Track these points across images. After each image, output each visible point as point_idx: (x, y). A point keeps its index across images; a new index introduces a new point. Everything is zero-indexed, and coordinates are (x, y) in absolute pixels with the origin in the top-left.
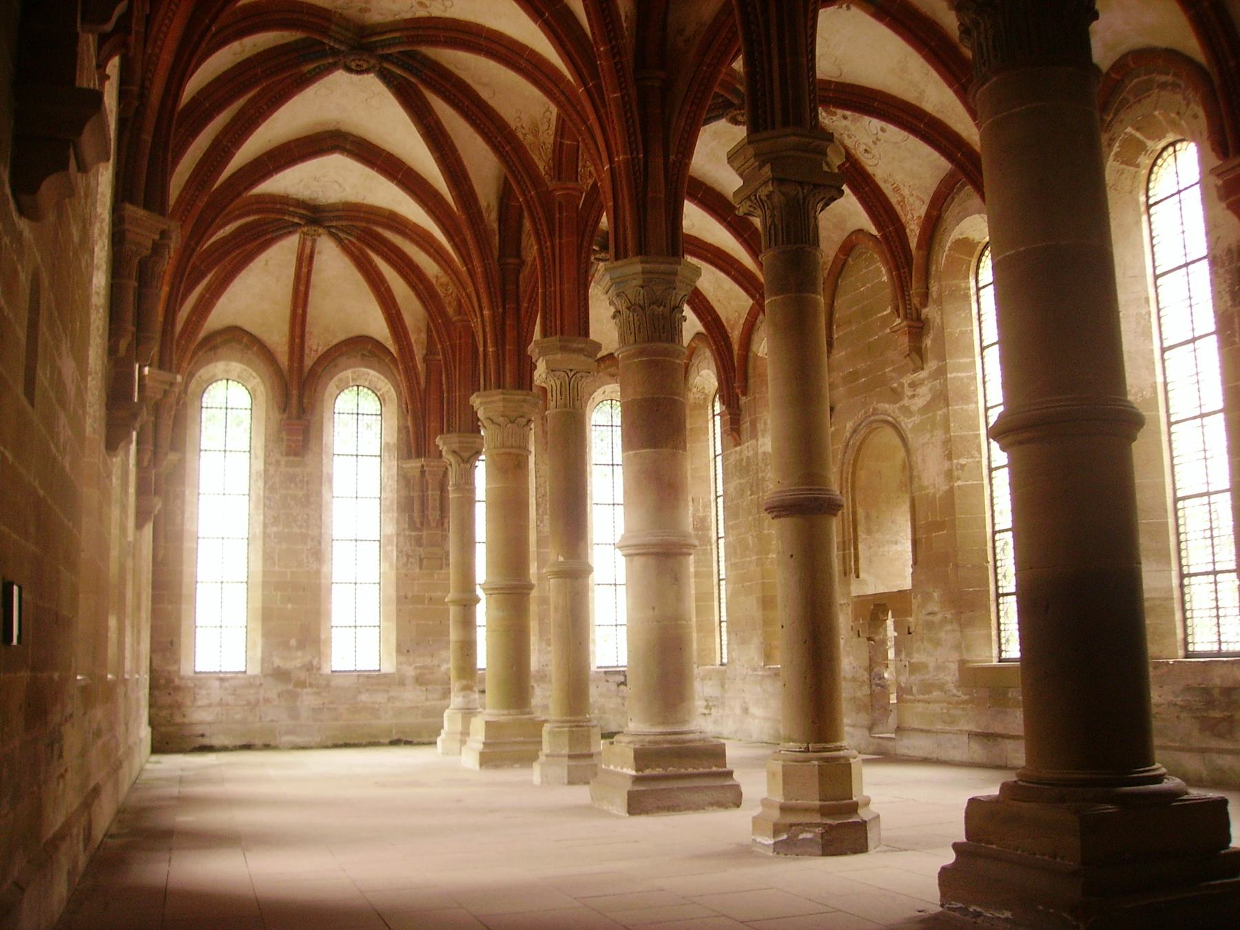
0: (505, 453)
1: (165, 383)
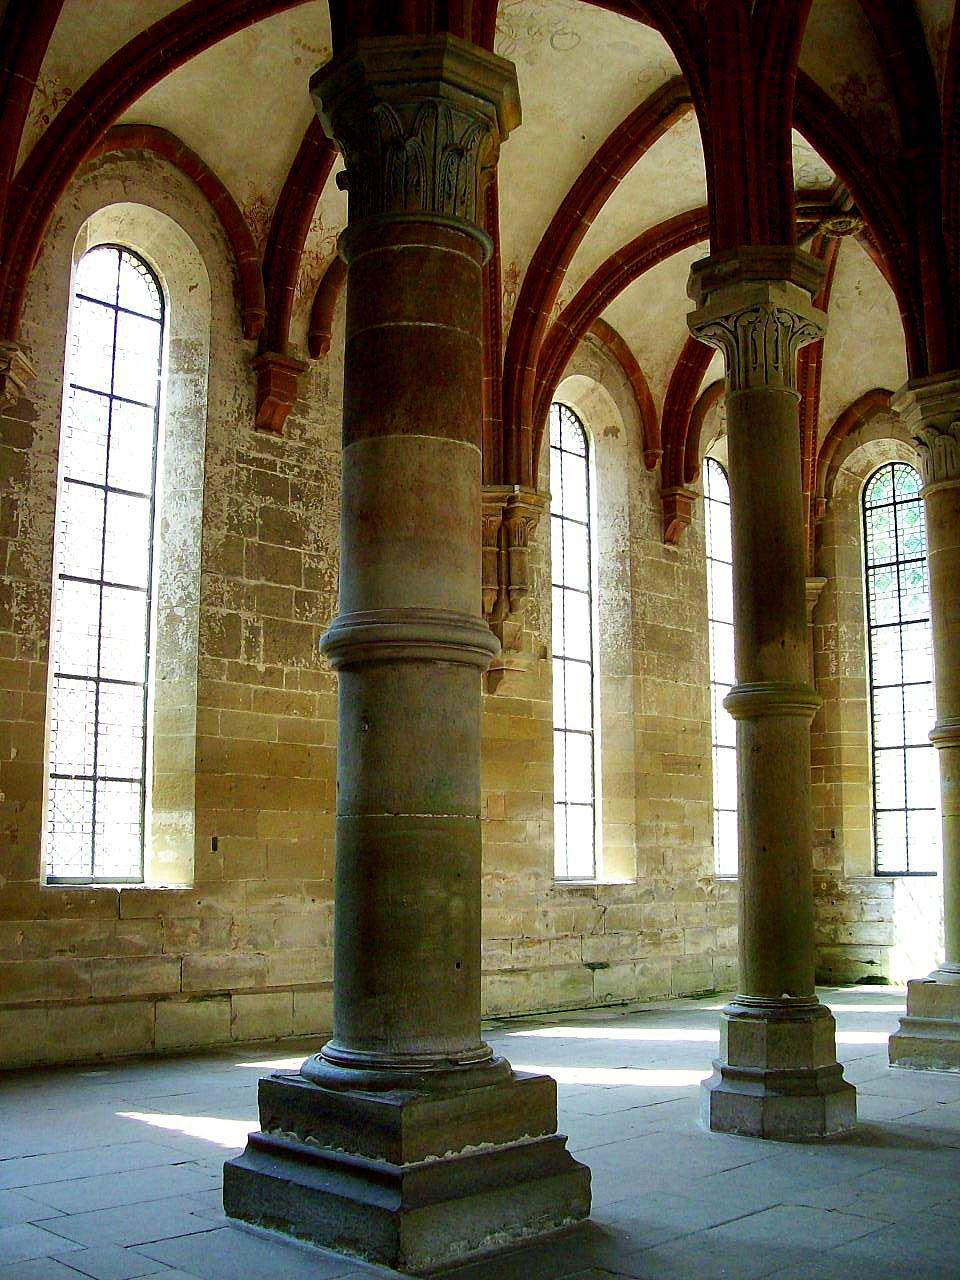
0: (938, 492)
1: (500, 500)
